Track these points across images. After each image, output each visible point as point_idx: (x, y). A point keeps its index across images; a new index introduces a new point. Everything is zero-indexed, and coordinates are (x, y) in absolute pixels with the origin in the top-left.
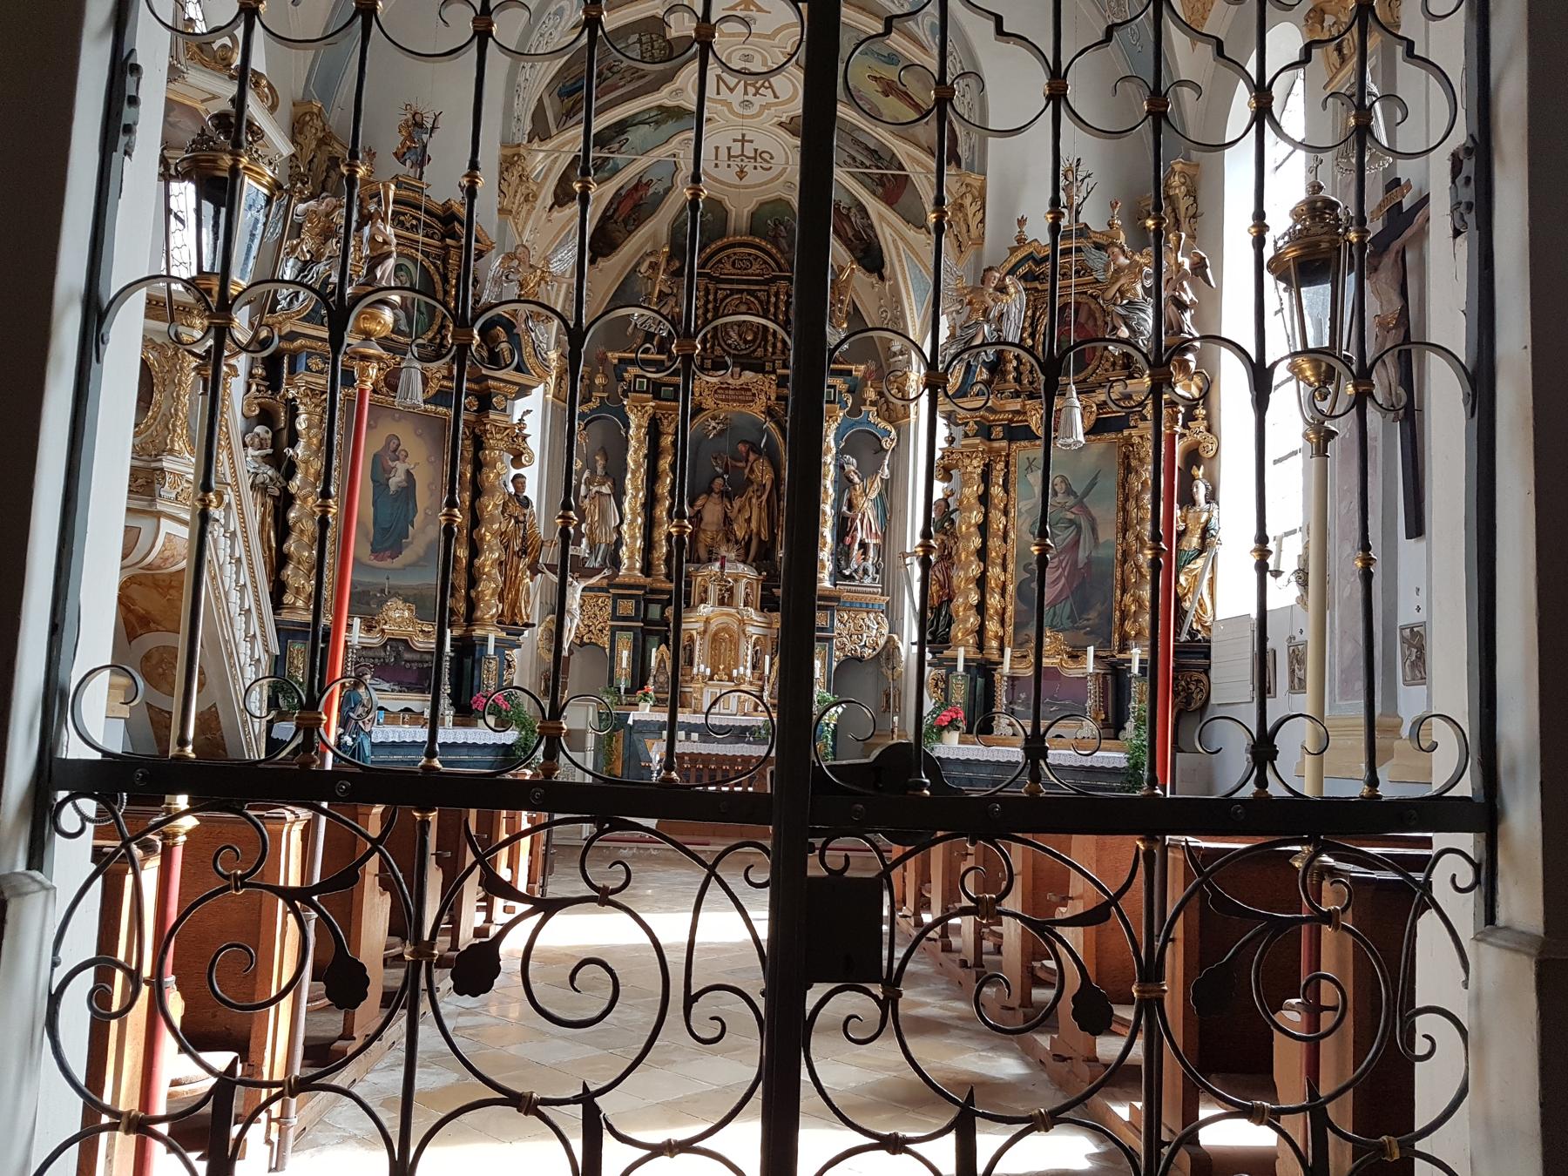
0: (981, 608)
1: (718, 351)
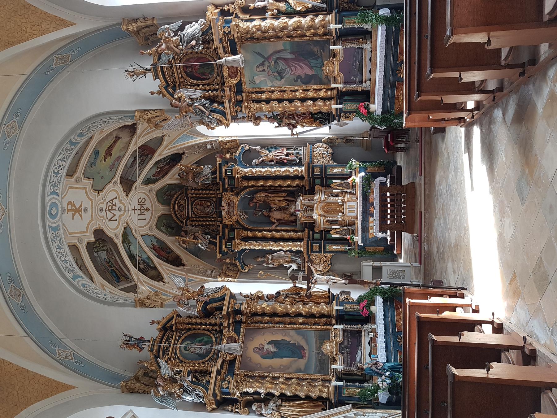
0: (314, 100)
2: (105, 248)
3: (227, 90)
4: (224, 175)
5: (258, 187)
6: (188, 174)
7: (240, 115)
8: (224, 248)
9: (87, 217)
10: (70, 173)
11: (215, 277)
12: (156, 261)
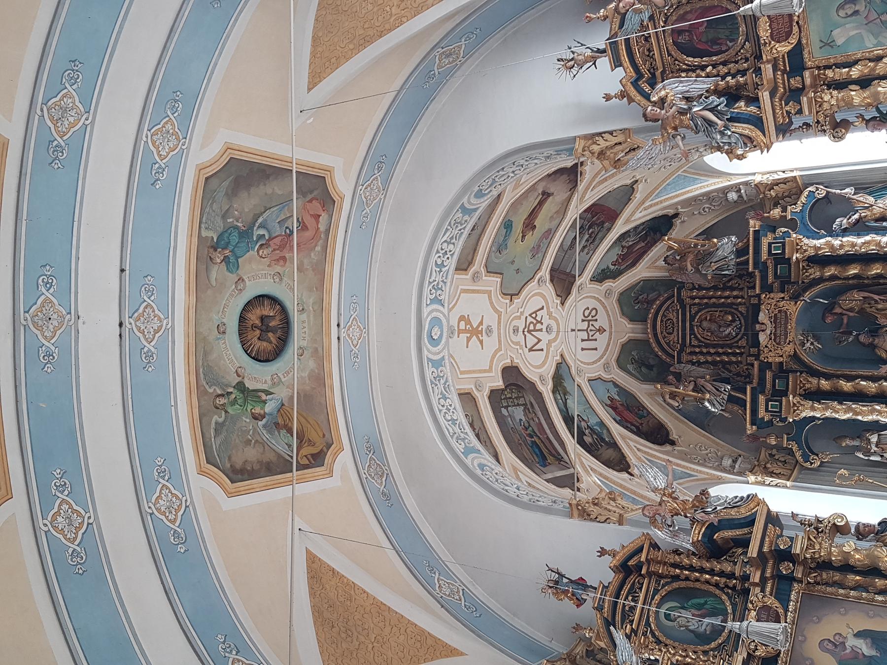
1: (743, 343)
2: (521, 401)
3: (767, 70)
4: (764, 256)
5: (847, 278)
6: (683, 256)
7: (797, 121)
8: (762, 413)
9: (491, 342)
10: (463, 266)
12: (617, 431)
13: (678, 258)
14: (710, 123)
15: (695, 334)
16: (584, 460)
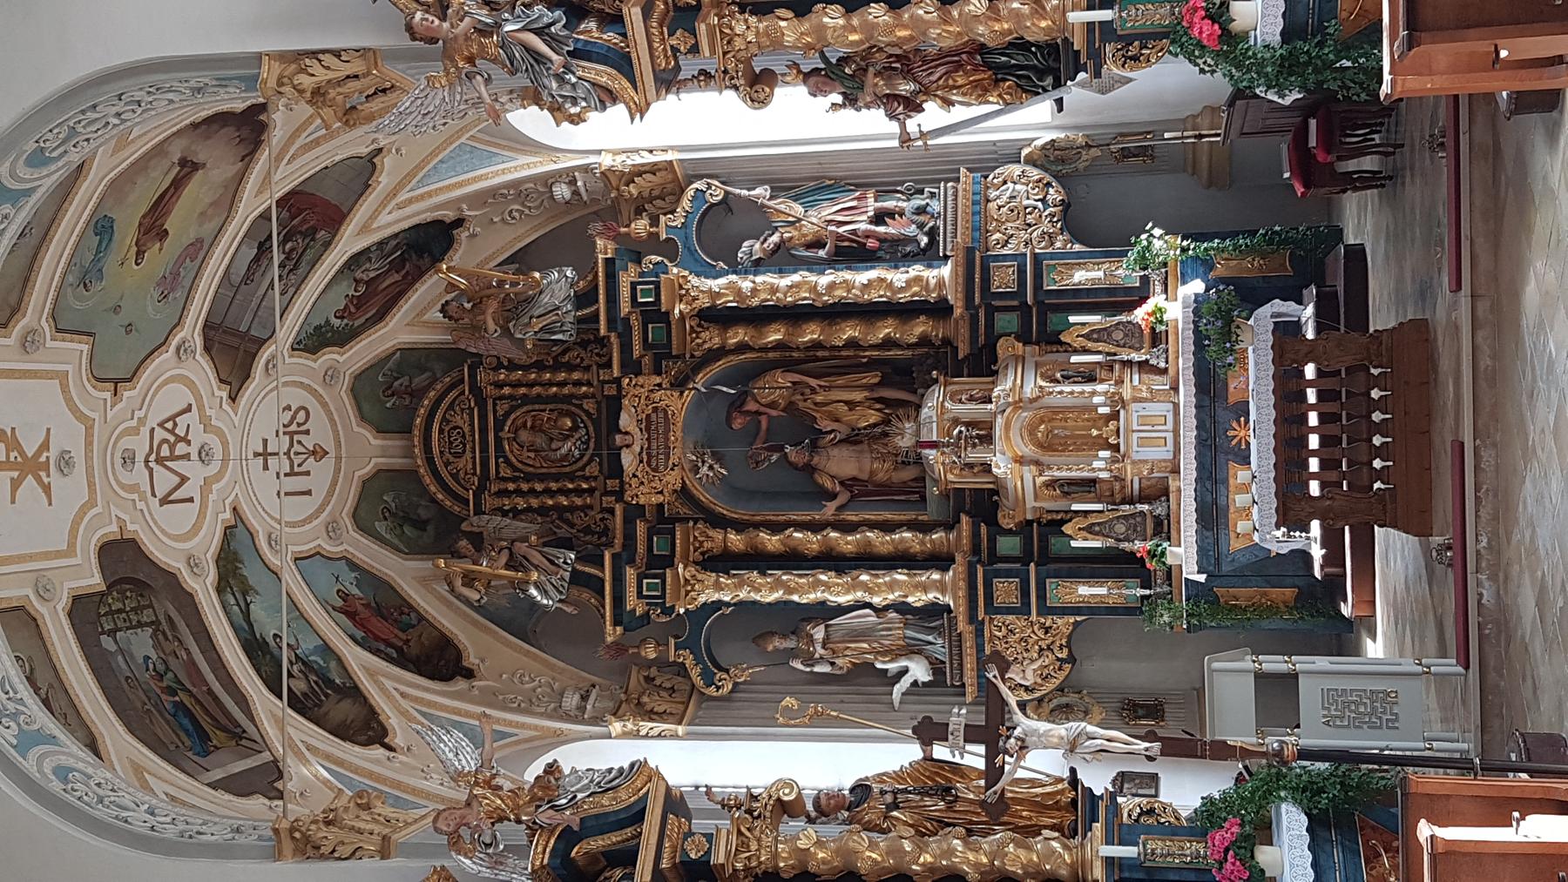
1: (593, 469)
2: (147, 616)
4: (625, 307)
5: (764, 349)
6: (479, 303)
7: (689, 67)
8: (631, 601)
9: (70, 489)
11: (597, 720)
12: (358, 660)
13: (468, 306)
14: (538, 58)
15: (506, 458)
16: (290, 730)
